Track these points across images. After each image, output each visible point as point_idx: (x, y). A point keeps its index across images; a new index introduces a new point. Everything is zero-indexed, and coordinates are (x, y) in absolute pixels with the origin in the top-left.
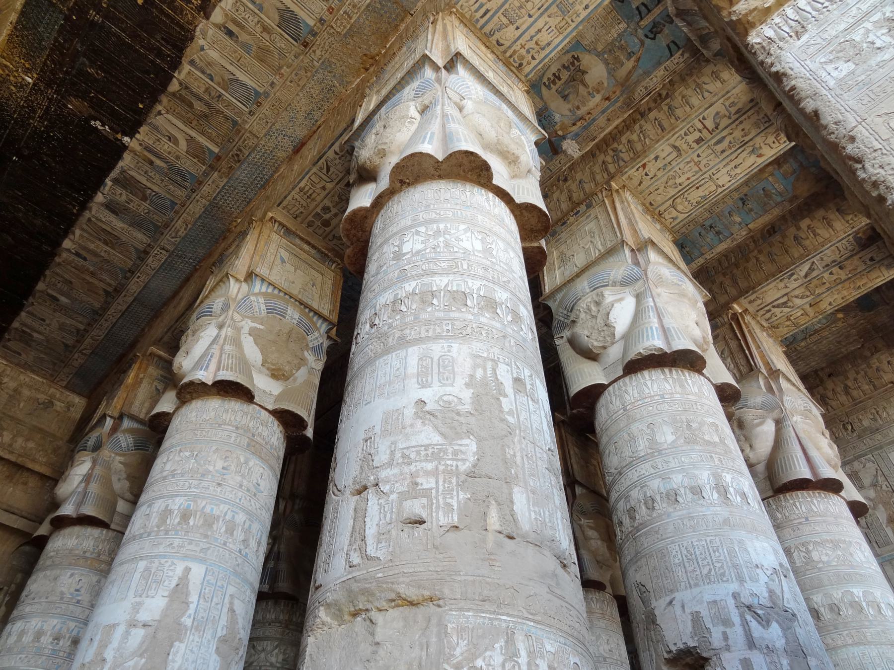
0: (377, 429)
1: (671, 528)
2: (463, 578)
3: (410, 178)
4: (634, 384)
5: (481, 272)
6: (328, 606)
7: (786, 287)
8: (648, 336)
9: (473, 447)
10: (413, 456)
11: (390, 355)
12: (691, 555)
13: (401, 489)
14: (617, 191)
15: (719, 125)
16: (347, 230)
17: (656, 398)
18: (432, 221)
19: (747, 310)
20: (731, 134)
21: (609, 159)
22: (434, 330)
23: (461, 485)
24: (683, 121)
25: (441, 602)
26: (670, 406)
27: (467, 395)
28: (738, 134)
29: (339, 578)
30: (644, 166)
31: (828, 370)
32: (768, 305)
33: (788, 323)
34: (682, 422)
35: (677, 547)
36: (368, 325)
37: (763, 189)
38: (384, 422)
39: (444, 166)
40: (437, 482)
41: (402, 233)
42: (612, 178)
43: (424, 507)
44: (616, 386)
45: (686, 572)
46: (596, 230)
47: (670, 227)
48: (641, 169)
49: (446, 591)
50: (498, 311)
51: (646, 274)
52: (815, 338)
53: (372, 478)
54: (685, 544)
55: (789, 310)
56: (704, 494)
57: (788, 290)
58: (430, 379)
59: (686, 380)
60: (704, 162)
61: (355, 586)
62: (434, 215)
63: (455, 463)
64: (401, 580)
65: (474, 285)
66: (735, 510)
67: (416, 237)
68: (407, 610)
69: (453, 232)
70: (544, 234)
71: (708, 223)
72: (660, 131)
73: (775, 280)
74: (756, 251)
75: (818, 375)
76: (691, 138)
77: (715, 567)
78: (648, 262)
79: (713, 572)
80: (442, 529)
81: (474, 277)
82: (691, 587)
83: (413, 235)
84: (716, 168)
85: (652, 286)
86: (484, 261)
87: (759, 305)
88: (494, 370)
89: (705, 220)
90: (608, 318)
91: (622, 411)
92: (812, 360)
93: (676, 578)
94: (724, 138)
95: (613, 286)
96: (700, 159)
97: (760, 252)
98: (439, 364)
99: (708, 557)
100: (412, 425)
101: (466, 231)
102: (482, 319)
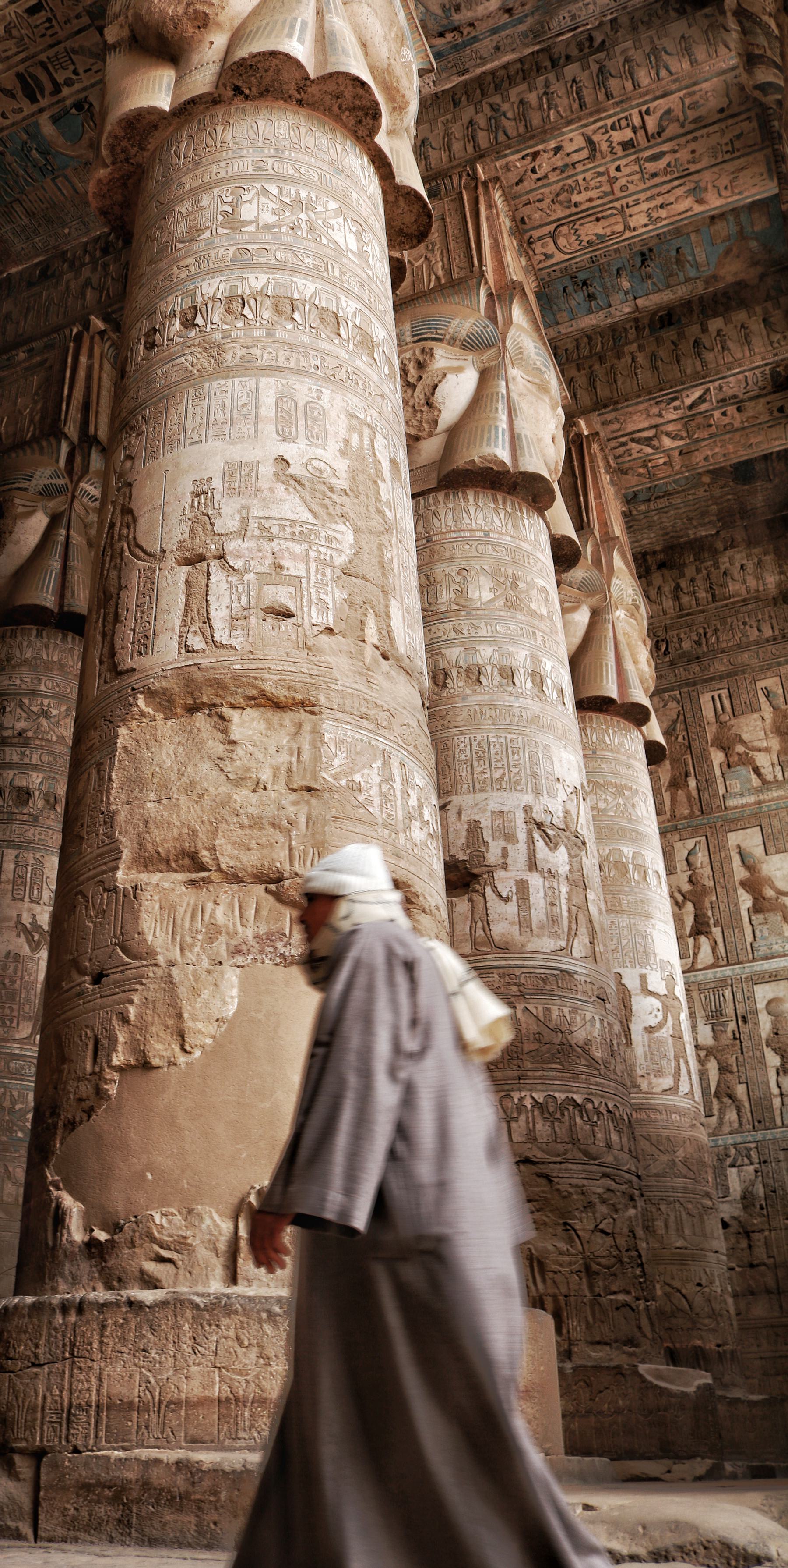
0: (217, 483)
1: (465, 714)
2: (340, 688)
3: (254, 89)
4: (451, 505)
5: (356, 289)
6: (150, 694)
7: (660, 415)
8: (489, 439)
9: (349, 537)
10: (275, 530)
11: (230, 381)
12: (484, 752)
13: (259, 569)
14: (485, 184)
15: (663, 131)
16: (116, 137)
17: (478, 534)
18: (287, 179)
19: (597, 434)
20: (675, 152)
21: (481, 120)
22: (298, 360)
23: (336, 580)
24: (617, 104)
25: (316, 709)
26: (495, 550)
27: (342, 465)
28: (684, 155)
29: (171, 663)
30: (535, 155)
31: (661, 557)
32: (626, 435)
33: (641, 470)
34: (507, 577)
35: (467, 740)
36: (178, 321)
37: (678, 250)
38: (227, 475)
39: (313, 89)
40: (308, 571)
41: (239, 182)
42: (482, 156)
43: (291, 597)
44: (422, 502)
45: (473, 774)
46: (438, 240)
47: (537, 267)
48: (529, 158)
49: (322, 700)
50: (376, 355)
51: (504, 341)
52: (662, 503)
53: (213, 547)
54: (479, 738)
55: (650, 450)
56: (516, 680)
57: (661, 421)
58: (293, 430)
59: (522, 518)
60: (623, 181)
61: (198, 675)
62: (291, 171)
63: (329, 552)
64: (267, 676)
65: (349, 307)
66: (548, 708)
67: (263, 200)
68: (269, 713)
69: (320, 209)
70: (415, 241)
71: (582, 276)
72: (576, 106)
73: (650, 399)
74: (635, 345)
75: (645, 561)
76: (618, 136)
77: (510, 772)
78: (509, 321)
79: (506, 778)
80: (316, 628)
81: (348, 292)
82: (475, 791)
83: (258, 193)
84: (635, 197)
85: (508, 361)
86: (360, 271)
87: (614, 432)
88: (372, 442)
89: (581, 270)
90: (433, 394)
91: (425, 541)
92: (645, 536)
93: (458, 778)
94: (662, 154)
95: (449, 344)
96: (618, 174)
97: (641, 348)
98: (306, 413)
99: (505, 759)
100: (271, 490)
101: (339, 212)
102: (359, 363)
